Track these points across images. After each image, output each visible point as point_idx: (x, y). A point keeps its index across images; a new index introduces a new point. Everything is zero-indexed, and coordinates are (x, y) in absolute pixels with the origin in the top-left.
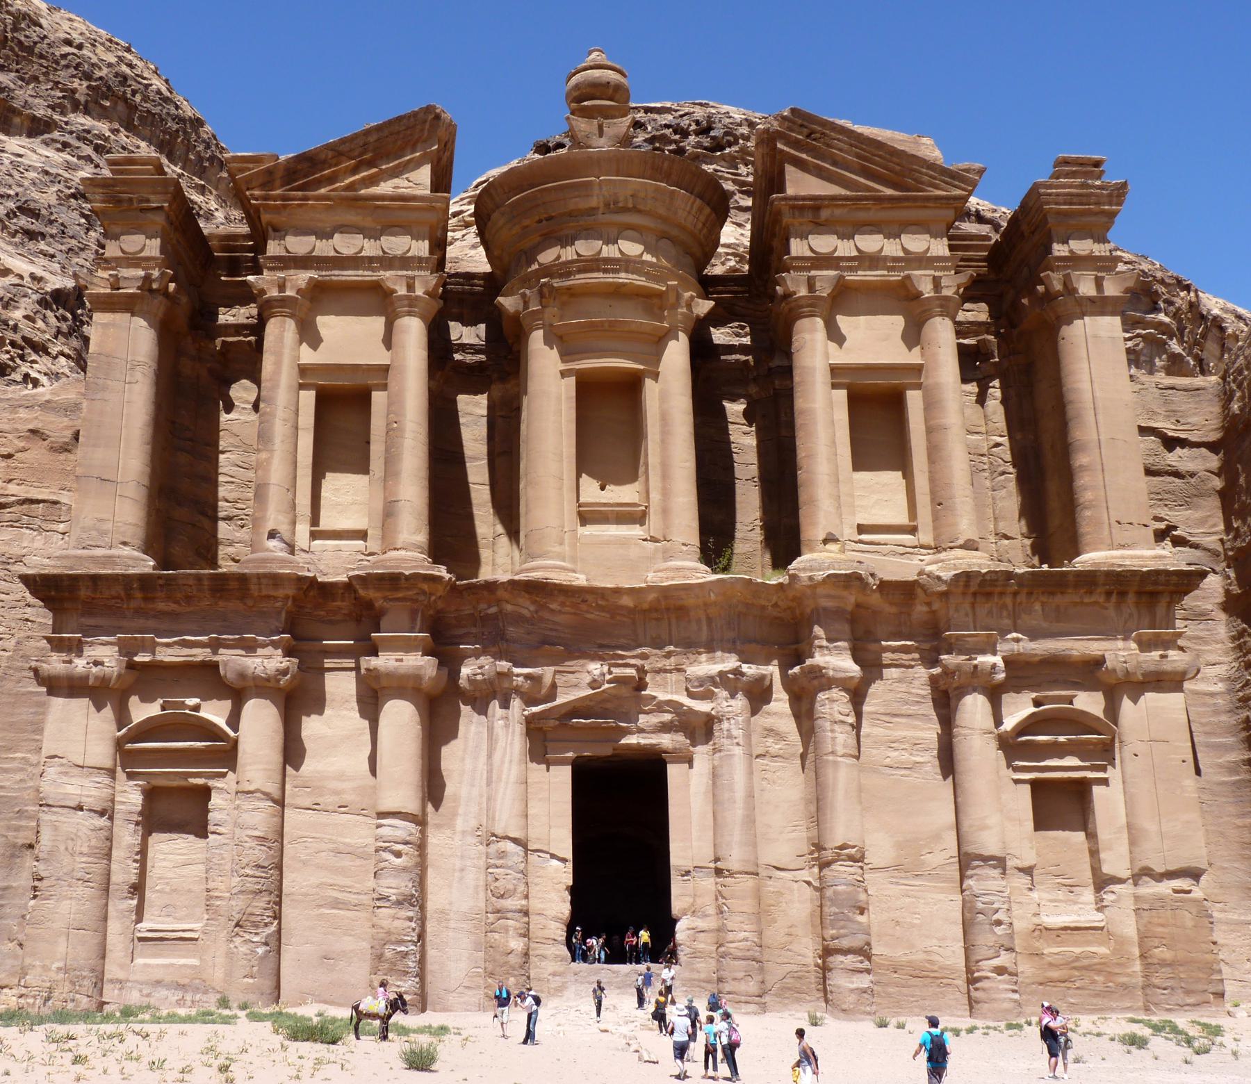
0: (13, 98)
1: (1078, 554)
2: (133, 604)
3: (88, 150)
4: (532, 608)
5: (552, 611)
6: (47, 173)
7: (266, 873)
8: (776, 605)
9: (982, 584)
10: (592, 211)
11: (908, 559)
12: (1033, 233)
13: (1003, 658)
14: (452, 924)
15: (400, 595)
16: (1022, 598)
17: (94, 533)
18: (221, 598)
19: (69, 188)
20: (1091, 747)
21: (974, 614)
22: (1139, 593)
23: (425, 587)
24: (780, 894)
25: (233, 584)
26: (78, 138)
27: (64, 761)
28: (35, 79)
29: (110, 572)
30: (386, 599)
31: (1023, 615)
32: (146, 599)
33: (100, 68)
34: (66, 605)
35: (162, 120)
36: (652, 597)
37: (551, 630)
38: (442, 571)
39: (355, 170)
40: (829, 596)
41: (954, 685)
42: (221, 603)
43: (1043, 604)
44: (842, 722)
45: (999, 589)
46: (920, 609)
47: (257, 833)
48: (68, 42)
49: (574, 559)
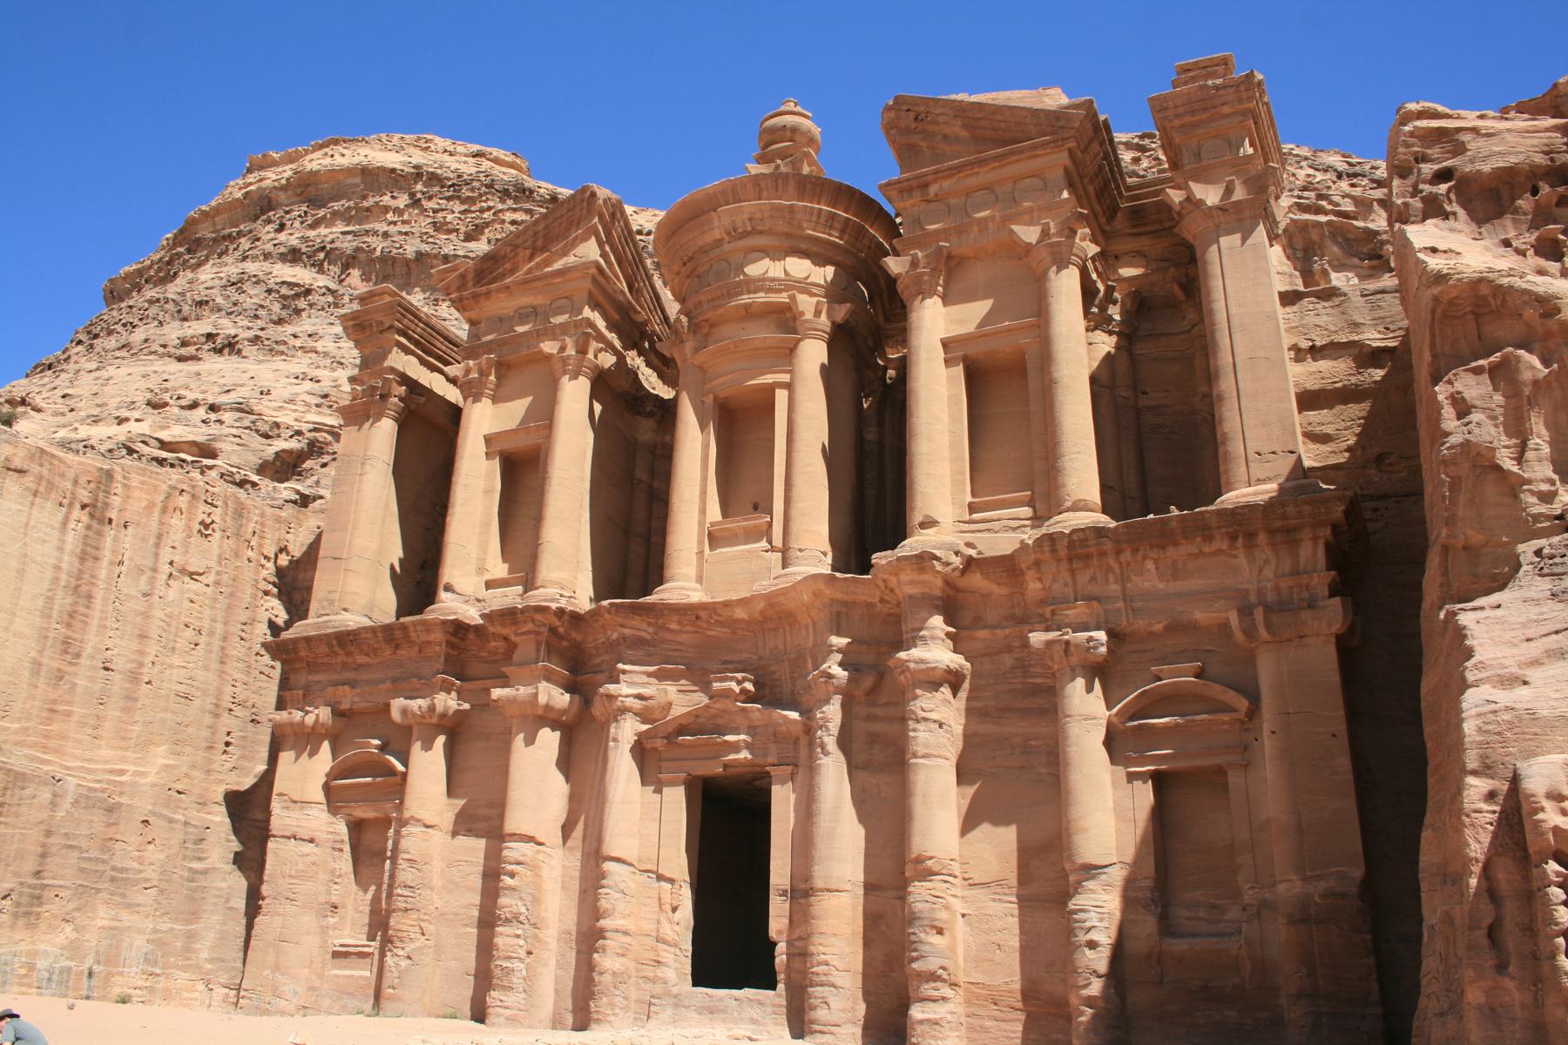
2: (340, 659)
4: (651, 630)
5: (673, 631)
7: (414, 892)
8: (882, 601)
9: (1071, 545)
11: (1024, 533)
15: (525, 629)
16: (1126, 556)
17: (325, 603)
18: (397, 647)
20: (1226, 727)
21: (1075, 584)
22: (1271, 532)
27: (286, 798)
30: (516, 634)
31: (1133, 578)
36: (761, 605)
37: (675, 650)
40: (912, 583)
41: (1056, 667)
42: (400, 652)
44: (926, 719)
46: (1033, 586)
47: (408, 856)
49: (700, 579)
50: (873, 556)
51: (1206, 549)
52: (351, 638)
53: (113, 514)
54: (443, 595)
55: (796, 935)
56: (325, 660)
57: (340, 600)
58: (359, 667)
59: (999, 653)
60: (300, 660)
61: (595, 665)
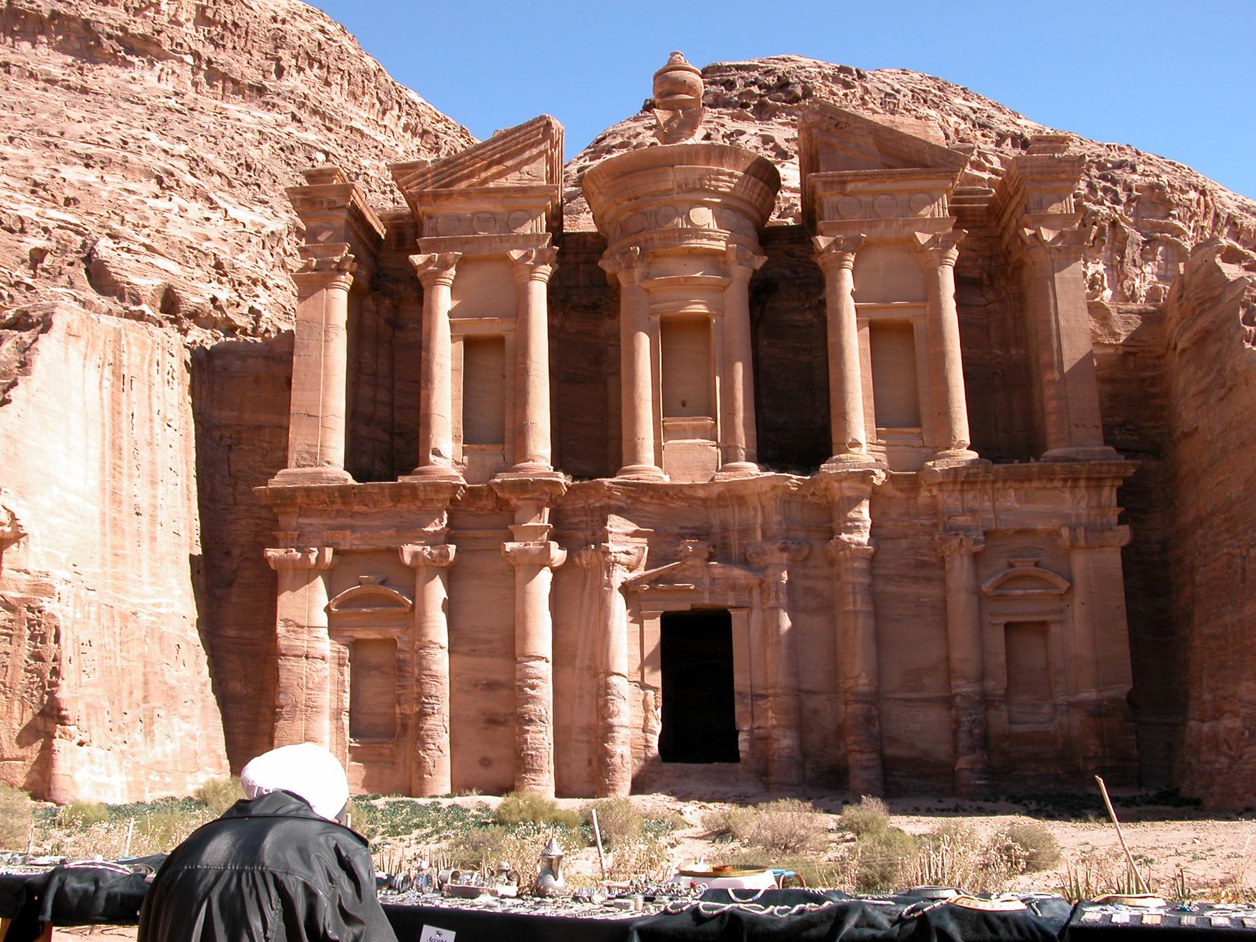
0: (231, 71)
1: (1046, 450)
2: (335, 507)
3: (292, 108)
4: (629, 501)
5: (645, 503)
6: (260, 132)
8: (813, 494)
10: (668, 192)
12: (1016, 193)
13: (985, 533)
14: (573, 736)
15: (527, 496)
18: (398, 501)
19: (278, 143)
21: (963, 500)
23: (547, 489)
24: (816, 712)
25: (406, 491)
26: (284, 99)
28: (249, 53)
29: (319, 485)
30: (518, 499)
32: (344, 503)
33: (300, 39)
34: (289, 509)
35: (349, 74)
38: (562, 478)
39: (488, 167)
40: (850, 488)
42: (399, 505)
43: (1016, 490)
45: (980, 479)
46: (924, 495)
48: (275, 19)
49: (658, 462)
50: (822, 466)
51: (1049, 486)
52: (356, 491)
53: (125, 371)
54: (432, 458)
55: (756, 725)
56: (320, 507)
57: (322, 454)
58: (353, 515)
59: (900, 538)
60: (293, 504)
61: (573, 524)
